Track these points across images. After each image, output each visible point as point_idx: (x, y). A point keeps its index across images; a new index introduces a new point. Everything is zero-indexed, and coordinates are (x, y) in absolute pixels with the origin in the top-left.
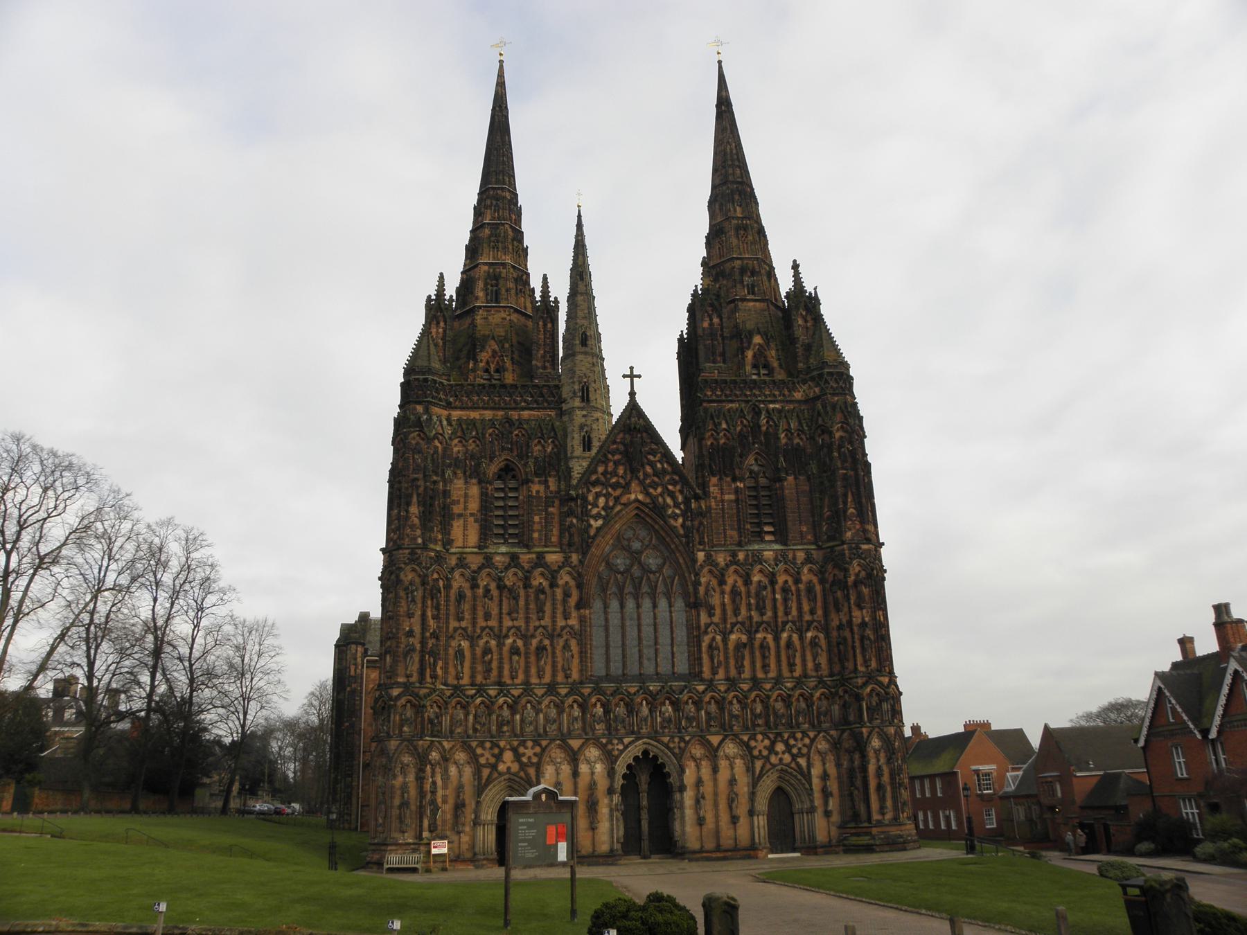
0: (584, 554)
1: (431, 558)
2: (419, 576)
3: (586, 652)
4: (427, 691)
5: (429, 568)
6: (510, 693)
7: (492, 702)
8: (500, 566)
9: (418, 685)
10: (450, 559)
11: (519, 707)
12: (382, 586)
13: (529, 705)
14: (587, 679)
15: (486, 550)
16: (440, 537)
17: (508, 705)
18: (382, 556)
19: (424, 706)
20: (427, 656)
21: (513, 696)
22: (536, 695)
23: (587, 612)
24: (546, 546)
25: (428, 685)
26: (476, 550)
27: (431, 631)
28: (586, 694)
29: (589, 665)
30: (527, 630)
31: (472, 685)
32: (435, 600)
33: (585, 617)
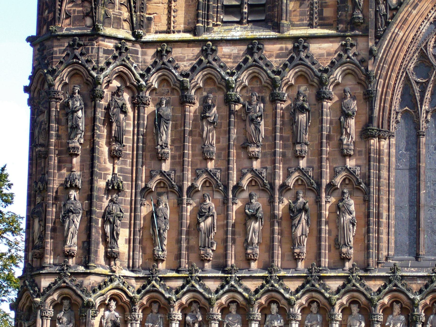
0: (379, 38)
1: (106, 52)
2: (87, 83)
3: (379, 215)
4: (99, 279)
5: (102, 70)
6: (240, 285)
7: (209, 300)
8: (231, 65)
9: (81, 269)
10: (144, 54)
11: (257, 313)
12: (30, 102)
13: (274, 307)
14: (378, 263)
15: (205, 36)
16: (126, 15)
17: (238, 305)
18: (31, 49)
19: (90, 306)
20: (100, 220)
21: (246, 290)
22: (287, 290)
23: (385, 143)
24: (311, 26)
25: (99, 270)
26: (188, 36)
27: (109, 177)
28: (376, 289)
29: (384, 237)
30: (273, 175)
31: (178, 271)
32: (114, 125)
33: (379, 152)
